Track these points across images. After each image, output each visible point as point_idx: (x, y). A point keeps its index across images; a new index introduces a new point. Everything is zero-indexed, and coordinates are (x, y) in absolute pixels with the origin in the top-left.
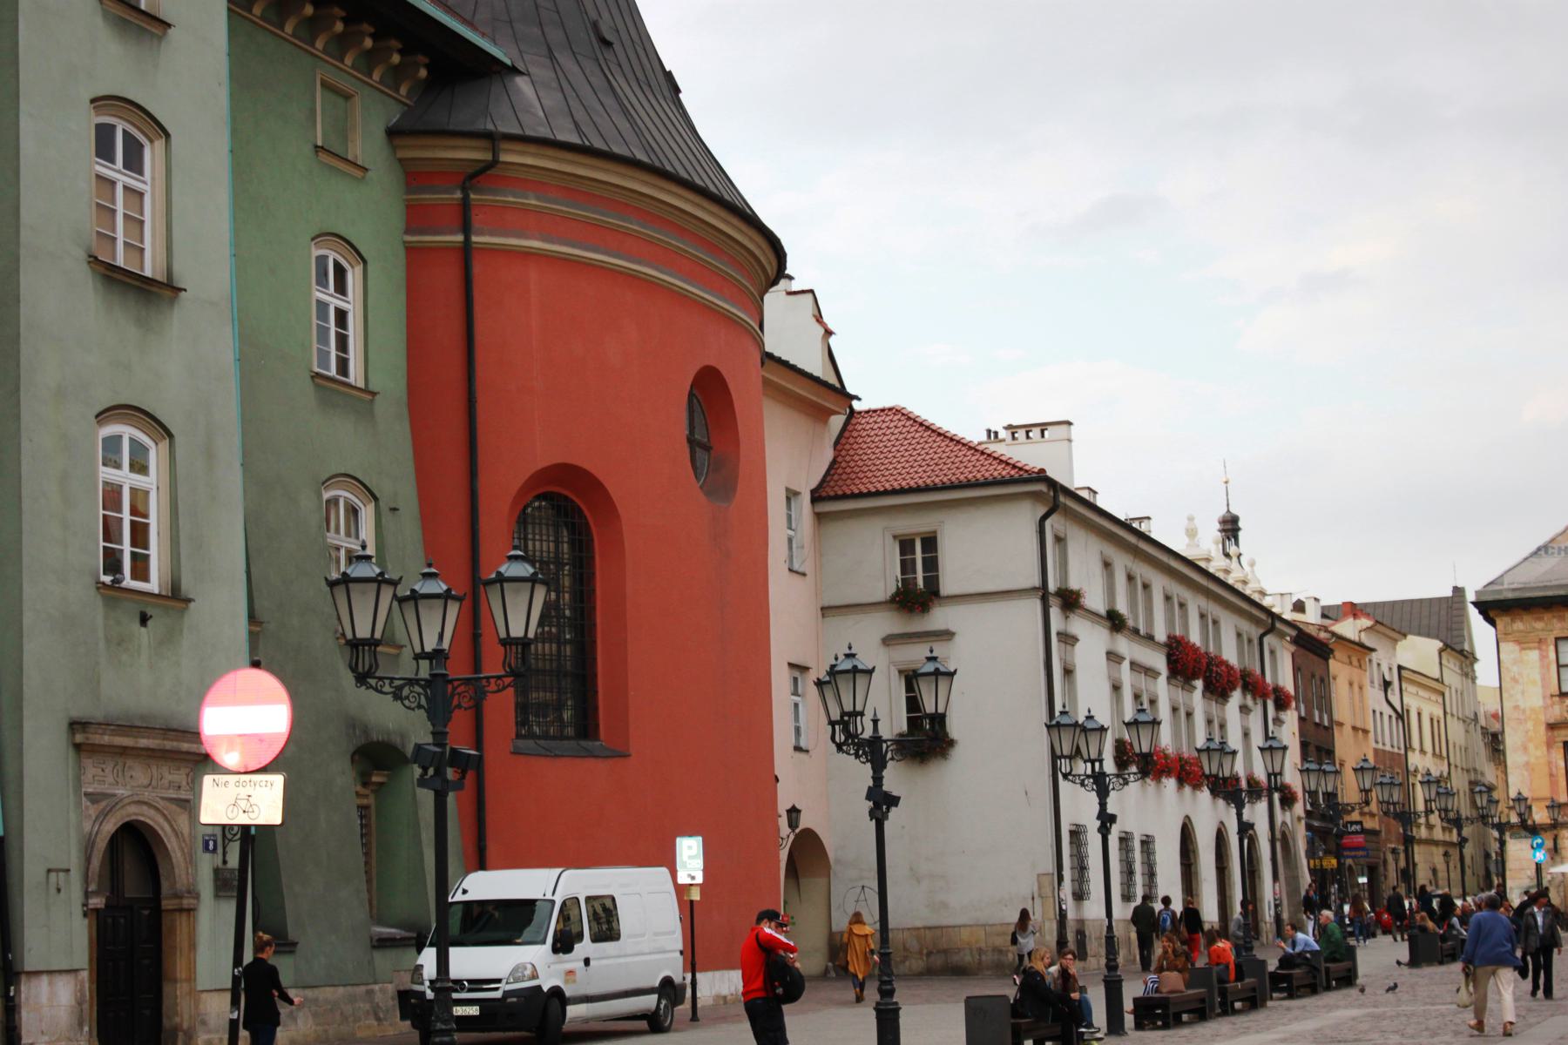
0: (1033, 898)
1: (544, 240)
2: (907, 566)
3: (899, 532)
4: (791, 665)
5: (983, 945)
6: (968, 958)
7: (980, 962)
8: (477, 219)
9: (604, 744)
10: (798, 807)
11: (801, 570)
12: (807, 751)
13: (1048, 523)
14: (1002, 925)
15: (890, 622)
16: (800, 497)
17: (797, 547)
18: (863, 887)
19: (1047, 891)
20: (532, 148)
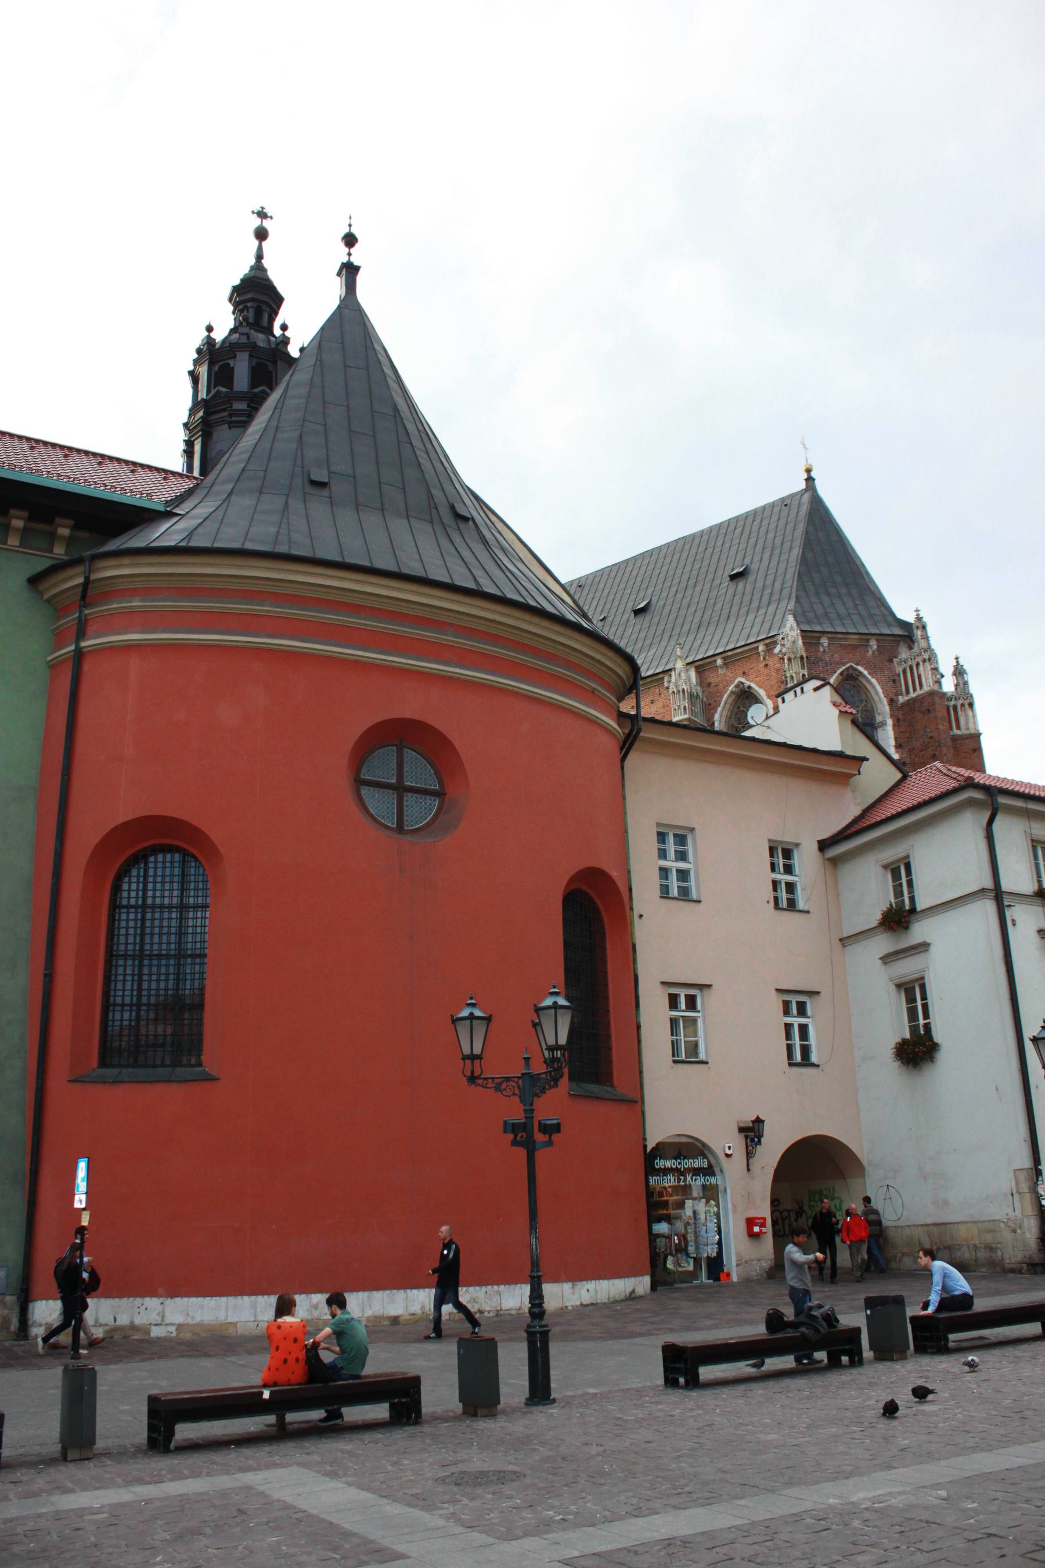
0: (1012, 1194)
1: (143, 632)
2: (898, 892)
3: (885, 862)
4: (779, 991)
5: (977, 1242)
6: (967, 1255)
7: (976, 1260)
8: (91, 628)
9: (207, 1069)
10: (762, 1118)
11: (806, 908)
12: (818, 1066)
13: (996, 826)
14: (990, 1221)
15: (883, 944)
16: (800, 847)
17: (802, 890)
18: (888, 1186)
19: (1025, 1187)
20: (126, 560)
